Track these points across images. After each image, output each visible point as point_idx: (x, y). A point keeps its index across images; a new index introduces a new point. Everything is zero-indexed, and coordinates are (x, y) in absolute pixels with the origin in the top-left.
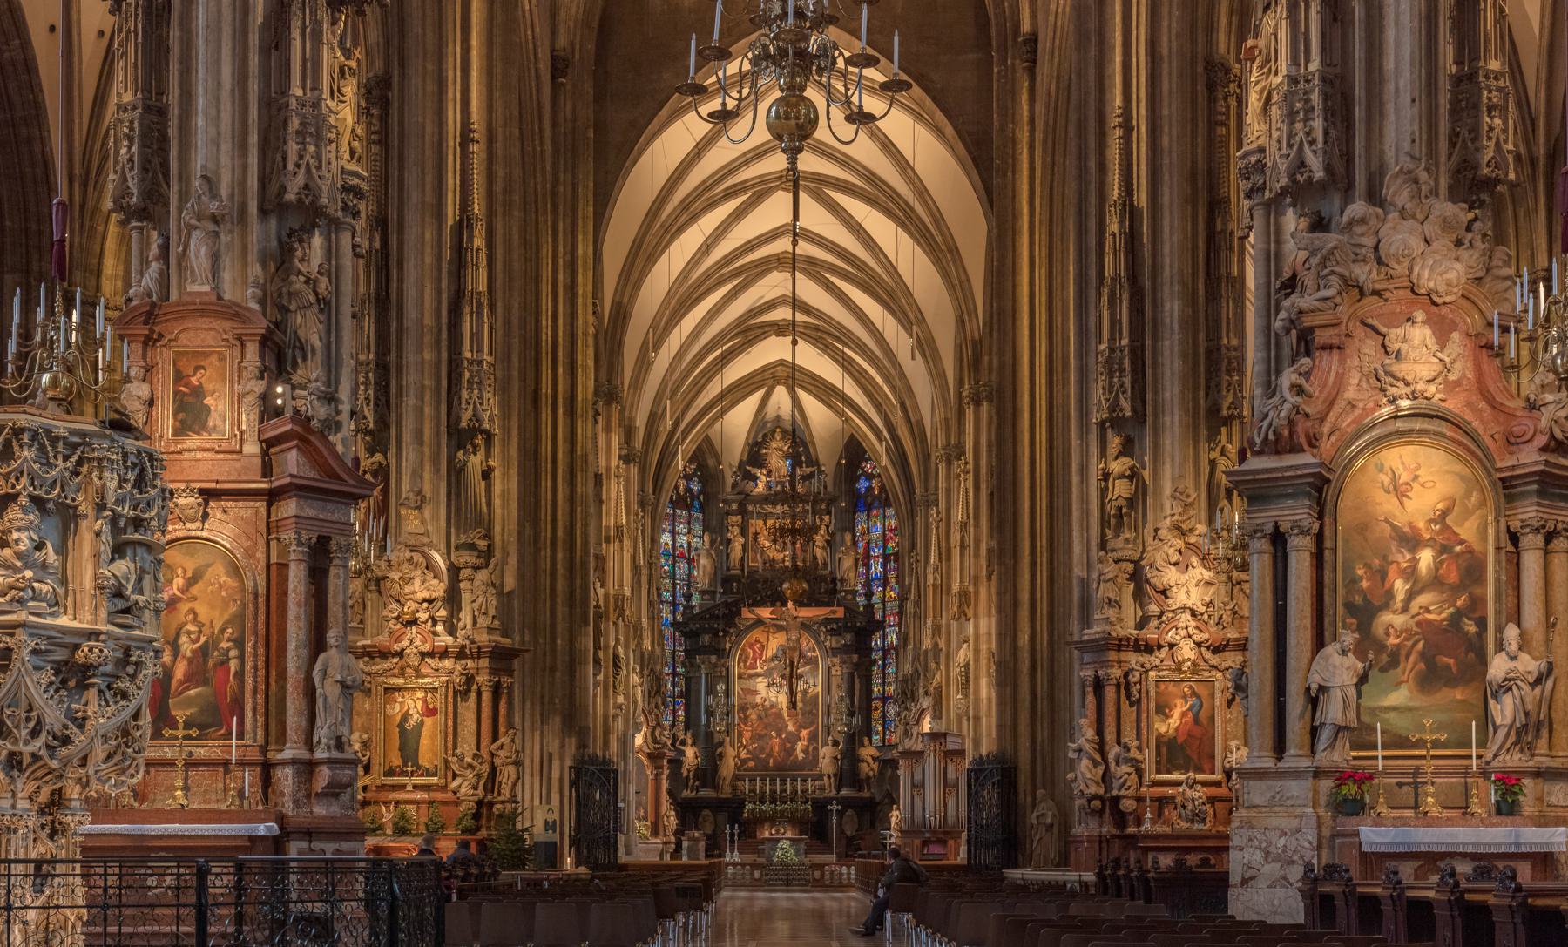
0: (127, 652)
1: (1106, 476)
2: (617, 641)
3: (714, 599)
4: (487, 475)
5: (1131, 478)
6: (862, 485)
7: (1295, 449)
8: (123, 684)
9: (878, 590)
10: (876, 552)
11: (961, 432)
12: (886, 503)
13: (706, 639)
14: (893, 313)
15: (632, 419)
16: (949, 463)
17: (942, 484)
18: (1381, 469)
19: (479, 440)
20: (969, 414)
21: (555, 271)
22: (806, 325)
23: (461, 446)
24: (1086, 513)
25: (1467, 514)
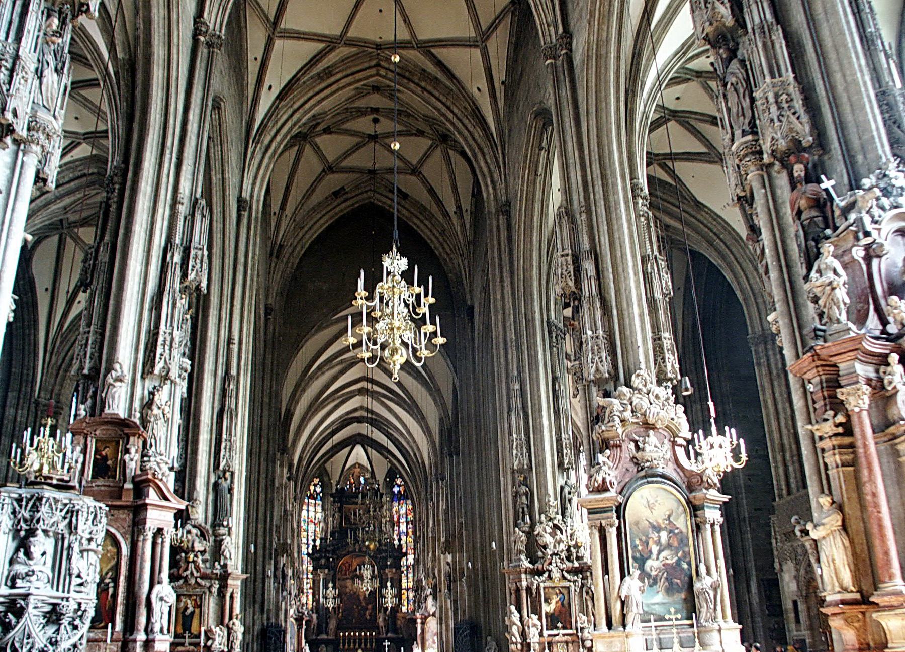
0: (80, 604)
1: (516, 495)
2: (284, 565)
3: (326, 542)
4: (230, 490)
5: (526, 494)
6: (396, 489)
7: (607, 490)
8: (77, 622)
9: (404, 538)
10: (403, 520)
11: (443, 468)
12: (406, 498)
13: (323, 561)
14: (411, 415)
15: (292, 460)
16: (438, 482)
17: (435, 491)
18: (642, 497)
19: (228, 474)
20: (447, 461)
21: (262, 397)
22: (371, 418)
23: (219, 478)
24: (507, 510)
25: (678, 516)
